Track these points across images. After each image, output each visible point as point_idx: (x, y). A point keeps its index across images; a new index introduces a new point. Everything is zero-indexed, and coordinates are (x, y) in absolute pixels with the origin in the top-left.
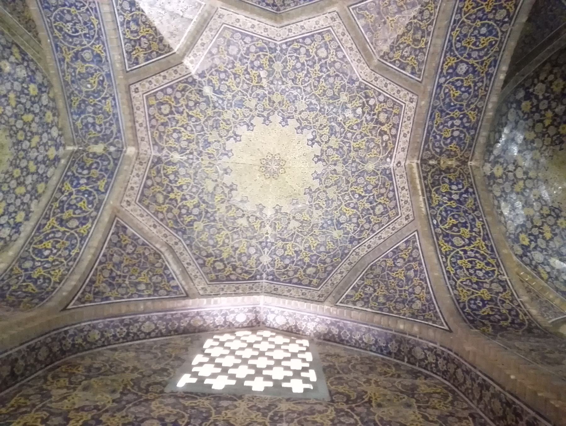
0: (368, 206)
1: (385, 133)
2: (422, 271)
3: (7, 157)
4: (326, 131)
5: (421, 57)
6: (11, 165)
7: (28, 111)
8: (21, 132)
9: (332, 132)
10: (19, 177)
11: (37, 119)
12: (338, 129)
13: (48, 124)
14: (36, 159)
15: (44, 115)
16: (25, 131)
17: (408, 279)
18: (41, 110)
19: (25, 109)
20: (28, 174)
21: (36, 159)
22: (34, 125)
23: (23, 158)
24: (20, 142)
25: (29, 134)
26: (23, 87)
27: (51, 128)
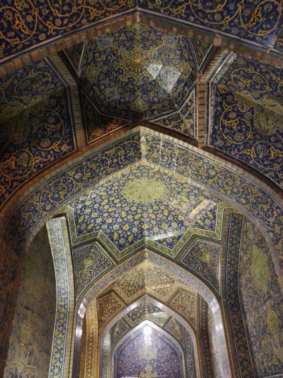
0: (131, 284)
1: (157, 287)
2: (112, 314)
3: (143, 201)
4: (159, 271)
5: (177, 307)
6: (138, 204)
7: (170, 212)
8: (158, 208)
9: (158, 273)
10: (131, 211)
11: (164, 218)
12: (160, 274)
13: (161, 225)
14: (142, 217)
15: (166, 223)
16: (158, 210)
17: (109, 311)
18: (169, 221)
19: (171, 211)
20: (133, 215)
21: (142, 217)
22: (161, 216)
23: (142, 210)
24: (152, 207)
25: (156, 213)
26: (183, 214)
27: (158, 227)
